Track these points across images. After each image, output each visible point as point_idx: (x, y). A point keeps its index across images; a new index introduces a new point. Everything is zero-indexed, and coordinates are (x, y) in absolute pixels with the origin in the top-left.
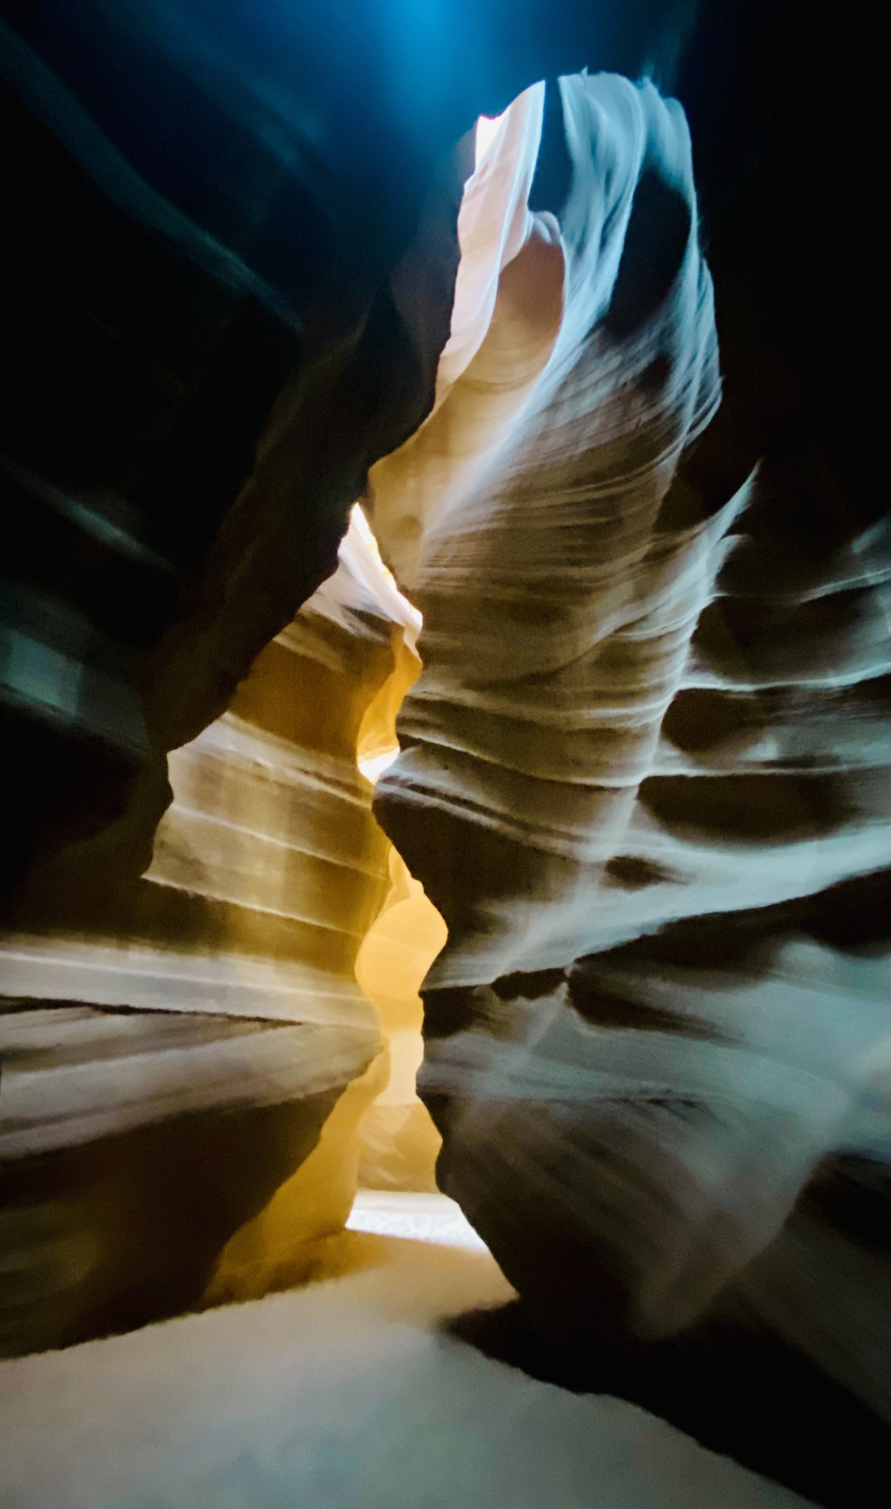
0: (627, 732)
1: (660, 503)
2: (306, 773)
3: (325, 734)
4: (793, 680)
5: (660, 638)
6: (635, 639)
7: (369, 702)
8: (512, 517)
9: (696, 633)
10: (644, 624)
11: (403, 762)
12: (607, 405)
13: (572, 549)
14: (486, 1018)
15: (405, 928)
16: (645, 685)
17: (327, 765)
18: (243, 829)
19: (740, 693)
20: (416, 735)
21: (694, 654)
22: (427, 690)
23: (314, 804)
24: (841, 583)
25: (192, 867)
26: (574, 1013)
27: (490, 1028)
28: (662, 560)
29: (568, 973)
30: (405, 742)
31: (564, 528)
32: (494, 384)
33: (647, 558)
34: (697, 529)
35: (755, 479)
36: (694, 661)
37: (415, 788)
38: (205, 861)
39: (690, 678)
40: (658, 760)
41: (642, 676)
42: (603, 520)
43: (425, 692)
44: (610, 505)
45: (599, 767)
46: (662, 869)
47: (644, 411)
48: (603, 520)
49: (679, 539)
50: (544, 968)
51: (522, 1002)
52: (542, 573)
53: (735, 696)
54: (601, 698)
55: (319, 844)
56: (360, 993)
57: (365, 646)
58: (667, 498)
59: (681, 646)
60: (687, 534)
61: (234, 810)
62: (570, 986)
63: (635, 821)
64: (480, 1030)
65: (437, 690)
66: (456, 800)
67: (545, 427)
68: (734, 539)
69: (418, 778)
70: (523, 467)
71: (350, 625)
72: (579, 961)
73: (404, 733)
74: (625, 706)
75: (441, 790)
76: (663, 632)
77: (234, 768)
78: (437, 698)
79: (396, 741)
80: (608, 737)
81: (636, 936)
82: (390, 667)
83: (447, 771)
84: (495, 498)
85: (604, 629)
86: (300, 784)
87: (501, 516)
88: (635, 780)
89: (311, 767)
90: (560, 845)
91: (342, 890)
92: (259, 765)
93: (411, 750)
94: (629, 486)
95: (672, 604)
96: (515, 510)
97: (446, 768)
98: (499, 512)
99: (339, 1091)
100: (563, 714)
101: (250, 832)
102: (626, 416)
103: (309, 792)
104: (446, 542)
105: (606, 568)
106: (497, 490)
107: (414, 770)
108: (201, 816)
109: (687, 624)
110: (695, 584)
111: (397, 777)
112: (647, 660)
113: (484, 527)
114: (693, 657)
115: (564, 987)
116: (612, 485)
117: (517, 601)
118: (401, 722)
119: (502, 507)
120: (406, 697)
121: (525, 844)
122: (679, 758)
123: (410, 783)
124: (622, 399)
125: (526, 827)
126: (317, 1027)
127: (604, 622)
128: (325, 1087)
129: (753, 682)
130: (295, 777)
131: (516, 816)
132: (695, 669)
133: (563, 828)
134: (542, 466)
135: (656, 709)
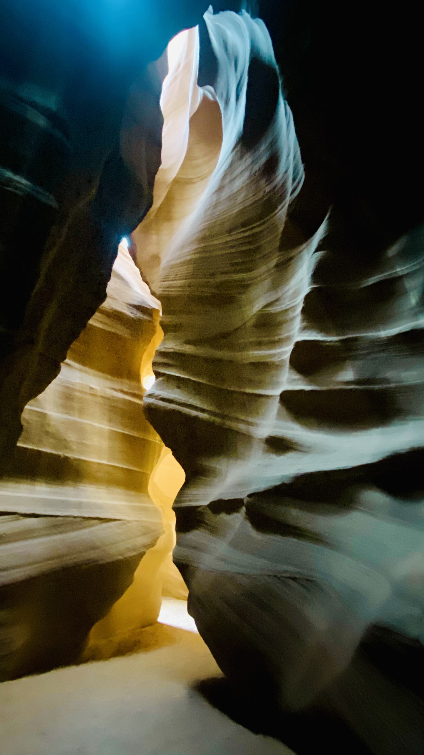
0: (273, 363)
1: (280, 236)
2: (116, 390)
3: (123, 370)
4: (359, 333)
5: (287, 310)
6: (272, 312)
7: (145, 350)
9: (303, 308)
10: (278, 303)
11: (157, 385)
12: (248, 184)
13: (237, 264)
14: (207, 524)
15: (167, 472)
16: (279, 337)
17: (126, 384)
19: (331, 342)
20: (162, 370)
21: (303, 320)
22: (166, 347)
24: (382, 275)
25: (63, 443)
26: (249, 524)
27: (208, 528)
28: (284, 267)
29: (245, 502)
30: (158, 374)
32: (192, 179)
33: (277, 266)
34: (301, 248)
35: (329, 218)
36: (305, 324)
38: (68, 439)
39: (302, 334)
40: (289, 381)
41: (279, 332)
42: (252, 247)
44: (254, 238)
45: (260, 384)
46: (292, 443)
47: (267, 186)
48: (252, 247)
49: (293, 254)
50: (233, 498)
51: (224, 516)
53: (327, 344)
54: (259, 344)
56: (151, 502)
57: (137, 324)
58: (283, 233)
59: (298, 315)
60: (296, 251)
61: (81, 412)
62: (247, 509)
63: (278, 414)
64: (204, 530)
65: (172, 346)
68: (320, 254)
72: (249, 496)
73: (157, 370)
74: (270, 349)
75: (176, 400)
76: (288, 307)
77: (79, 391)
78: (171, 350)
79: (153, 373)
80: (264, 367)
81: (278, 483)
82: (154, 332)
85: (257, 306)
86: (113, 397)
88: (278, 392)
89: (117, 387)
90: (242, 427)
91: (136, 450)
92: (92, 388)
93: (161, 379)
94: (263, 227)
95: (291, 291)
99: (142, 555)
102: (258, 189)
105: (255, 273)
107: (161, 390)
108: (66, 416)
109: (299, 302)
110: (302, 280)
111: (154, 394)
112: (280, 324)
114: (303, 322)
115: (244, 509)
116: (253, 228)
117: (209, 296)
118: (154, 364)
120: (157, 351)
121: (225, 427)
122: (298, 380)
123: (160, 397)
124: (255, 180)
125: (223, 417)
126: (129, 522)
127: (256, 303)
128: (134, 553)
129: (337, 335)
131: (217, 411)
132: (304, 329)
133: (243, 418)
135: (286, 351)
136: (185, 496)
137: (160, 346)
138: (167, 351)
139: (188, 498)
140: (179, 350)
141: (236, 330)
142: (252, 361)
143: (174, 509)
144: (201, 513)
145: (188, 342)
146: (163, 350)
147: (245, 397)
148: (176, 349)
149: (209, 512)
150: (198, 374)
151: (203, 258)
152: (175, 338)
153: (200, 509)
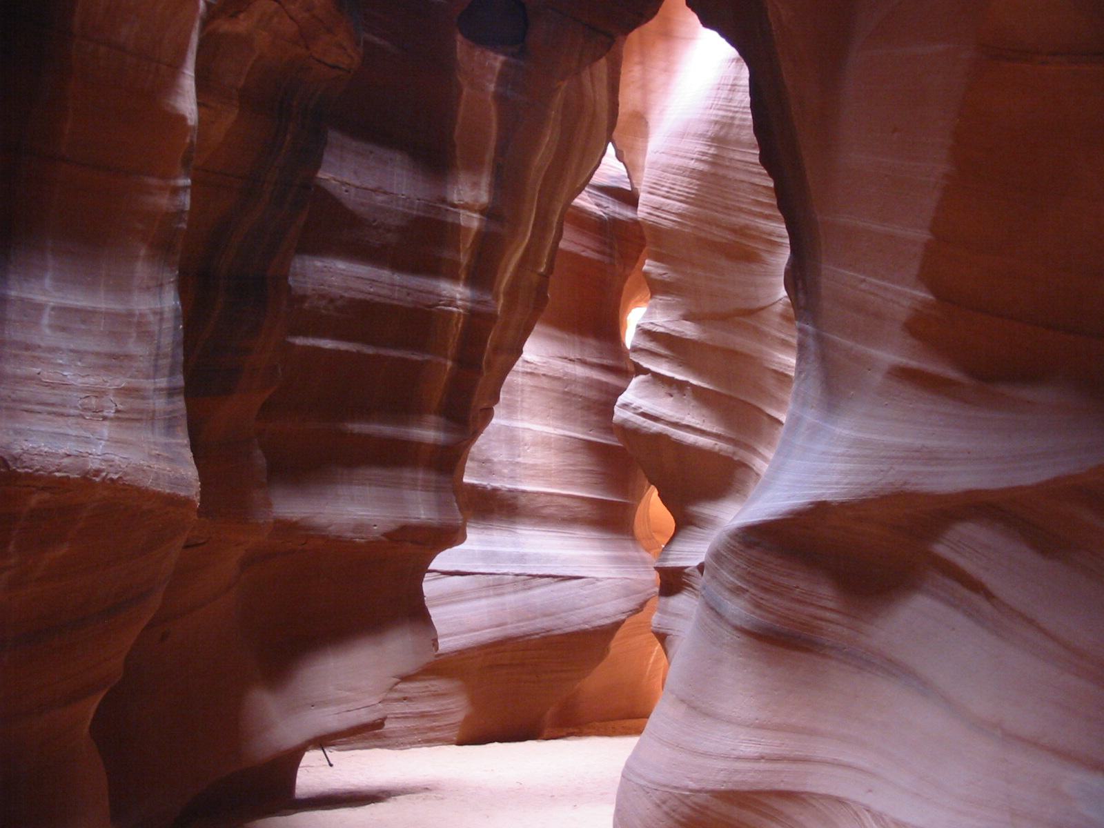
8: (716, 161)
18: (520, 424)
23: (579, 390)
31: (753, 184)
37: (644, 415)
43: (652, 323)
52: (743, 220)
55: (588, 425)
66: (676, 425)
67: (735, 79)
69: (648, 405)
70: (721, 113)
71: (598, 205)
83: (671, 399)
84: (702, 136)
87: (704, 158)
96: (714, 156)
97: (671, 396)
98: (704, 154)
100: (765, 349)
101: (527, 425)
103: (573, 381)
104: (666, 169)
106: (702, 128)
113: (693, 164)
119: (705, 149)
121: (736, 458)
130: (560, 367)
134: (733, 118)
136: (671, 552)
137: (644, 317)
138: (654, 330)
139: (675, 556)
140: (673, 331)
141: (762, 309)
142: (775, 367)
143: (657, 569)
144: (688, 575)
145: (686, 318)
146: (648, 327)
147: (765, 418)
148: (668, 329)
149: (697, 573)
150: (699, 371)
151: (714, 175)
152: (668, 307)
153: (686, 571)
